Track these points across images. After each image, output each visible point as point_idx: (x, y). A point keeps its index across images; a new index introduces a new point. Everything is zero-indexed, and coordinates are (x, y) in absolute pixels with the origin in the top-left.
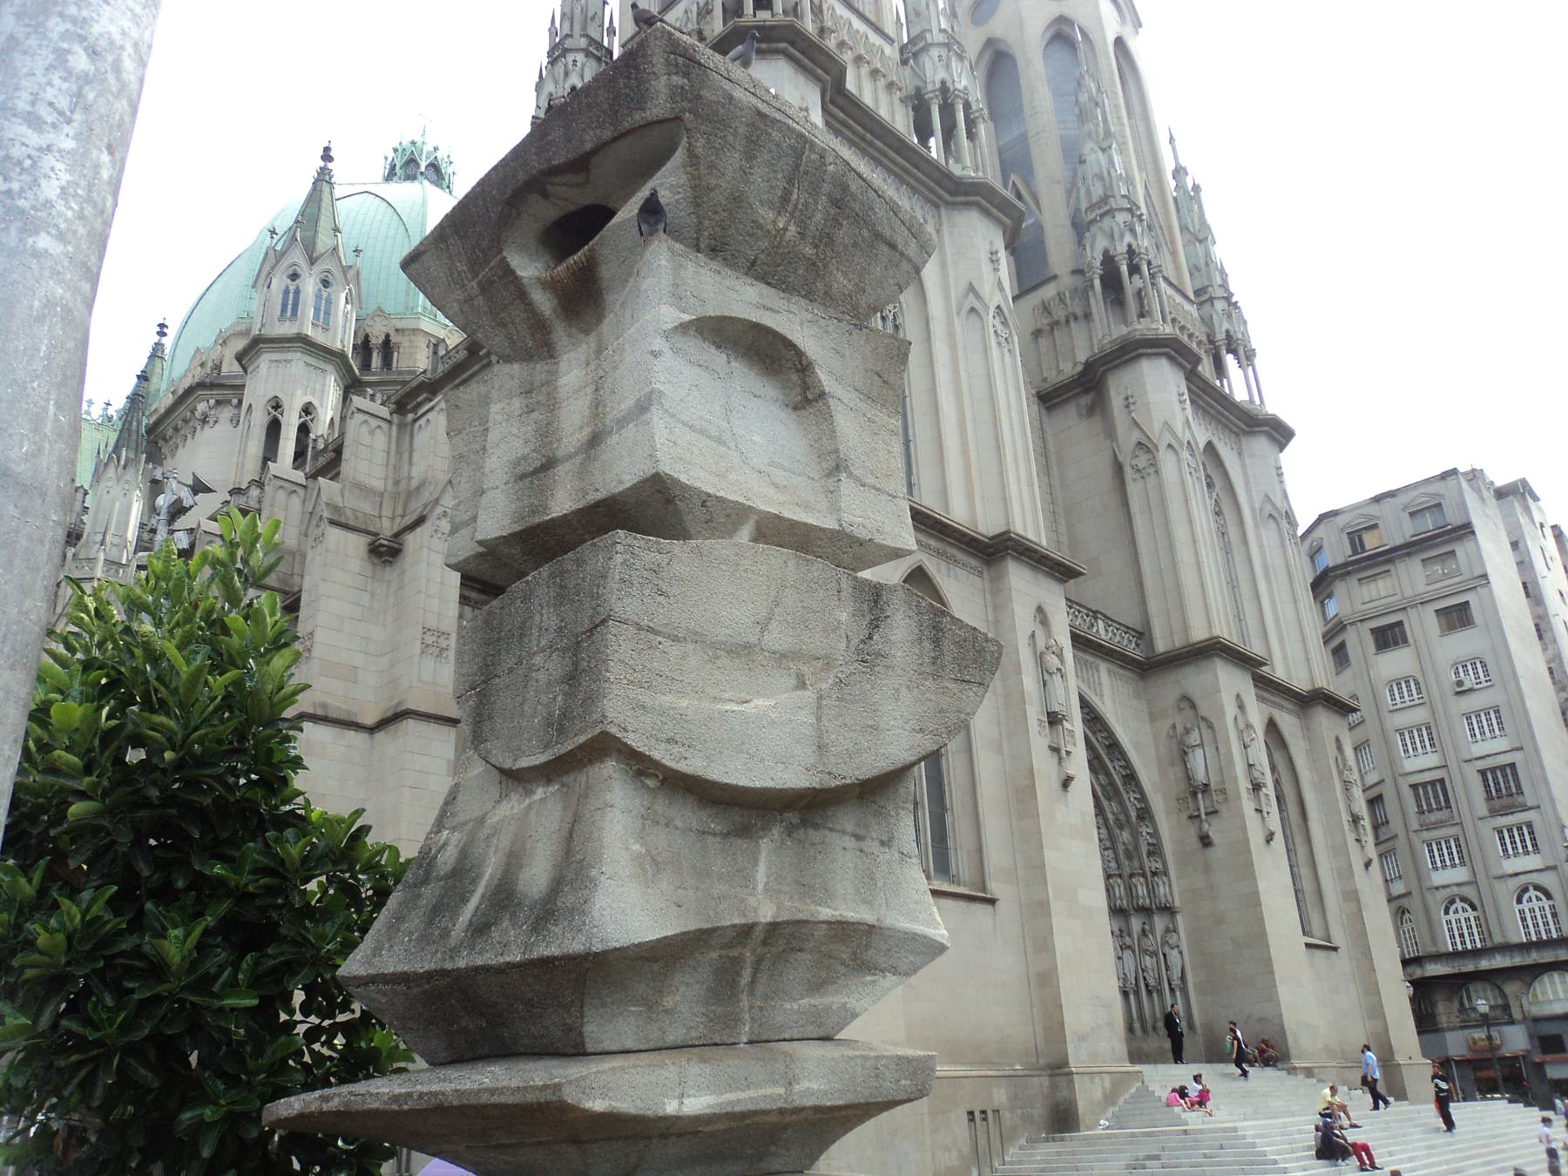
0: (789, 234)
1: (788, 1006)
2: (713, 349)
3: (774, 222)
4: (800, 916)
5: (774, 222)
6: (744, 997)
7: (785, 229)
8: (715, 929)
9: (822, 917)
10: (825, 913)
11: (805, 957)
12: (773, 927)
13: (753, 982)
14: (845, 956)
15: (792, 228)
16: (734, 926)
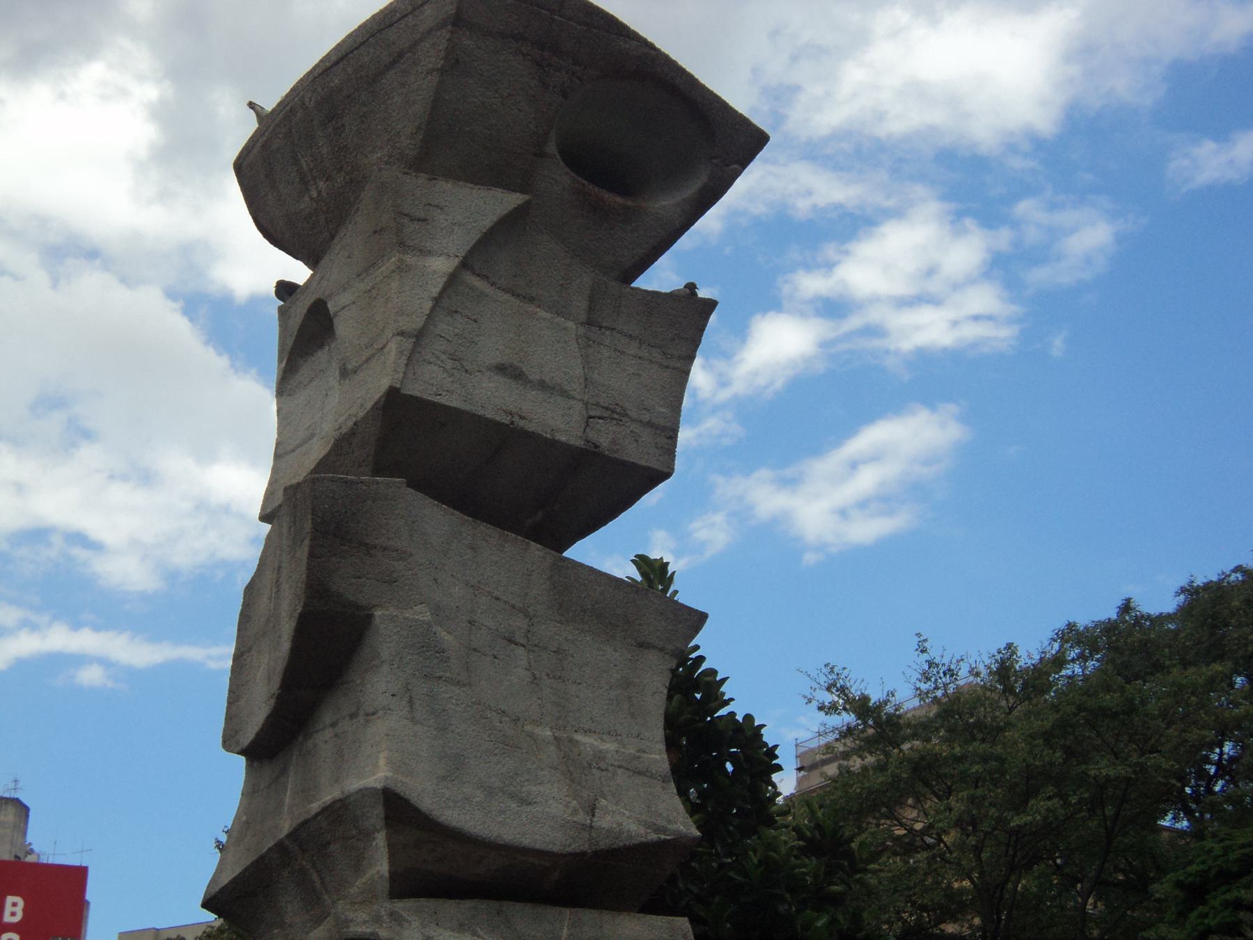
0: (324, 194)
1: (352, 891)
2: (320, 353)
3: (312, 199)
4: (302, 819)
5: (312, 199)
6: (326, 897)
7: (319, 193)
8: (262, 857)
9: (313, 812)
10: (315, 807)
11: (334, 847)
12: (294, 834)
13: (322, 883)
14: (354, 832)
15: (321, 184)
16: (270, 849)
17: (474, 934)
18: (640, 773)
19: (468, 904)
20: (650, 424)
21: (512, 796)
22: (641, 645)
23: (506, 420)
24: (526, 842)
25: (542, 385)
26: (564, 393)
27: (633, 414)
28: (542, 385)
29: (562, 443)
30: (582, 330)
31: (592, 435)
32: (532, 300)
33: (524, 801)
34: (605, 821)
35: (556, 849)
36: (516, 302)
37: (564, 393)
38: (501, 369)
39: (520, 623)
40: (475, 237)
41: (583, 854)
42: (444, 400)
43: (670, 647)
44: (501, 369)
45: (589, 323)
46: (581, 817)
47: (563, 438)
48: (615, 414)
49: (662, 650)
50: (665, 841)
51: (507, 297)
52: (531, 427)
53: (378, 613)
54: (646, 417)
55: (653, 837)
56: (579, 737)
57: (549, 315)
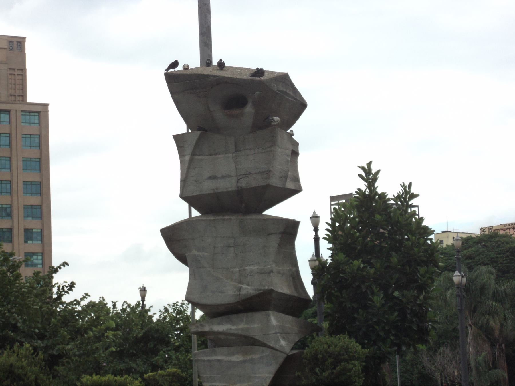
17: (223, 324)
18: (263, 273)
19: (220, 318)
20: (260, 173)
21: (220, 292)
22: (269, 235)
23: (212, 192)
24: (223, 303)
25: (223, 177)
26: (230, 176)
27: (253, 172)
28: (223, 177)
29: (230, 191)
30: (234, 155)
31: (239, 185)
32: (217, 154)
33: (223, 292)
34: (243, 292)
35: (231, 302)
36: (212, 157)
37: (230, 176)
38: (210, 178)
39: (232, 241)
40: (193, 147)
41: (238, 302)
42: (194, 194)
43: (278, 232)
44: (210, 178)
45: (236, 151)
46: (237, 293)
47: (230, 190)
48: (248, 174)
49: (276, 233)
50: (261, 293)
51: (209, 157)
52: (220, 191)
53: (186, 255)
54: (258, 171)
55: (257, 292)
56: (247, 268)
57: (223, 156)
